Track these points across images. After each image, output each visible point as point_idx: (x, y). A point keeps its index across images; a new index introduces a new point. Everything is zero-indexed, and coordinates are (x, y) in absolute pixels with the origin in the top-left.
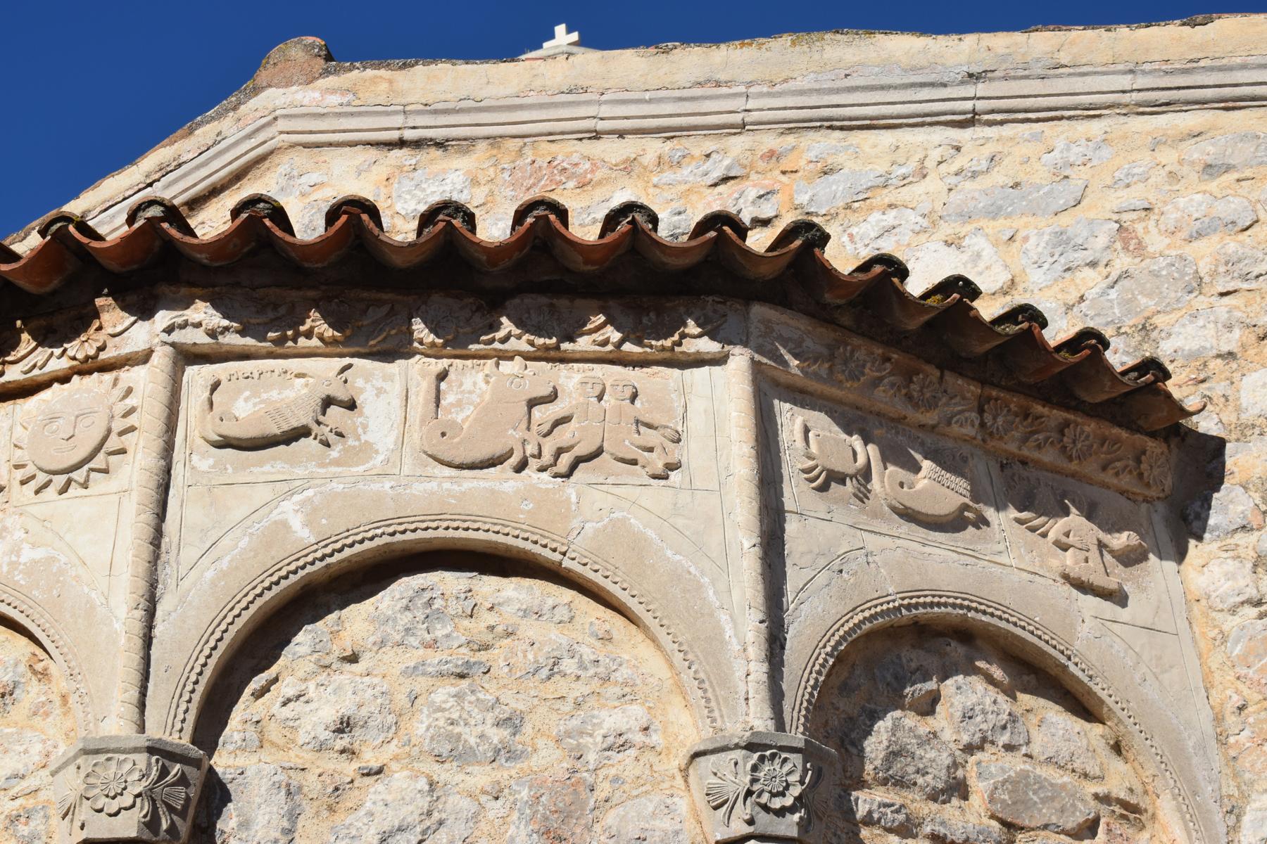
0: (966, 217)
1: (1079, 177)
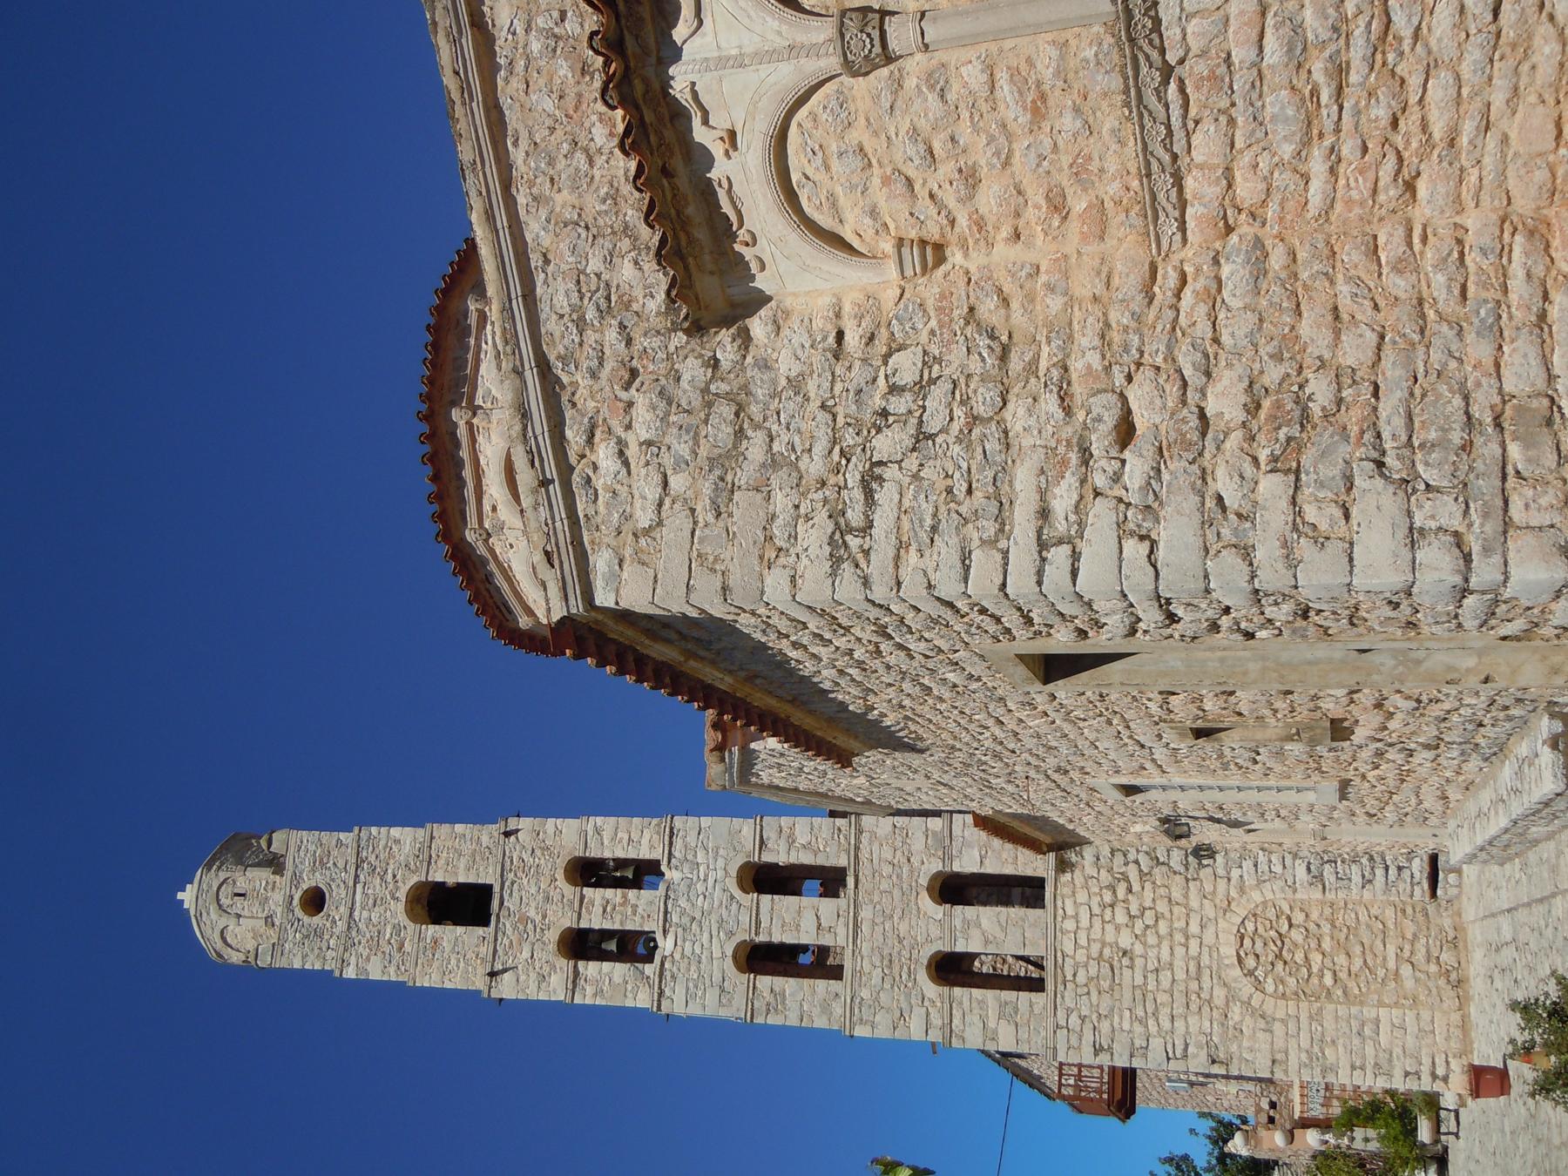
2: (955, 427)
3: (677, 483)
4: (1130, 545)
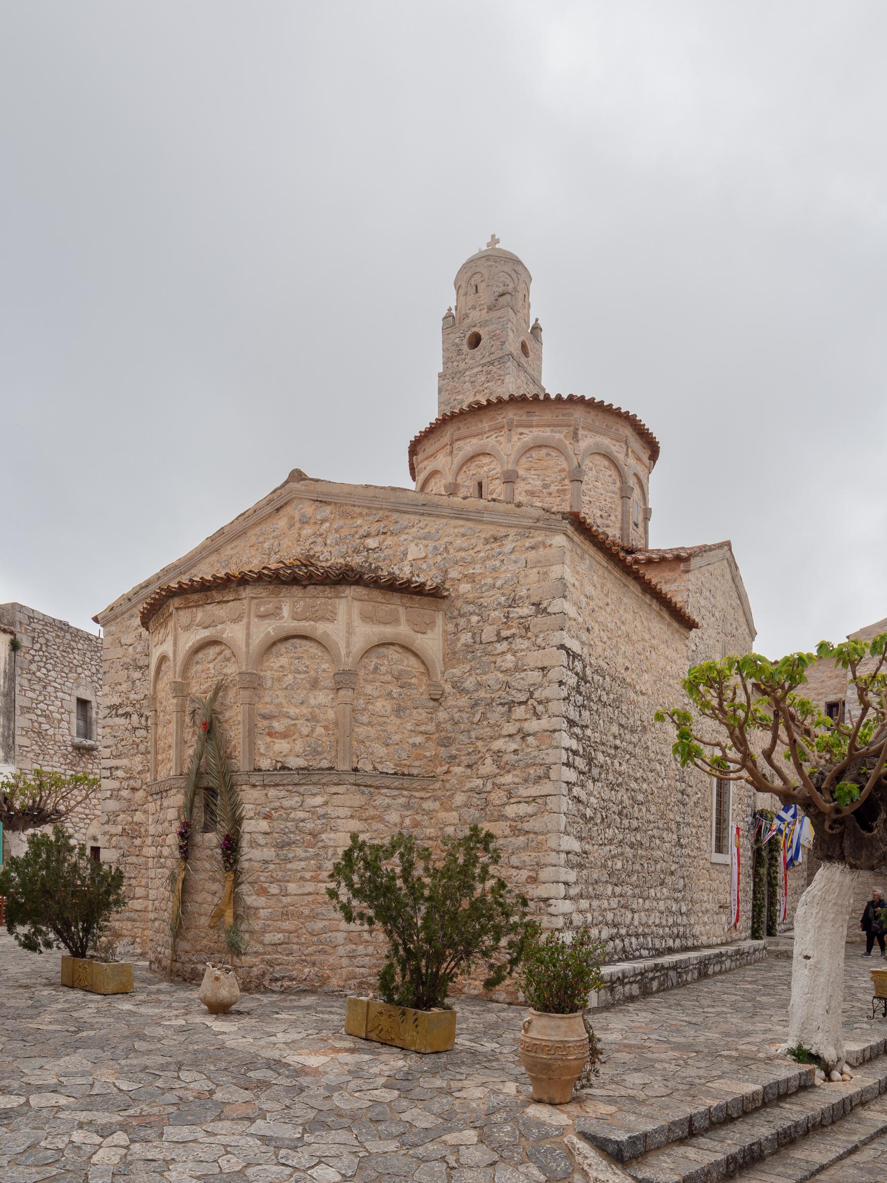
0: (420, 539)
1: (441, 532)
2: (136, 739)
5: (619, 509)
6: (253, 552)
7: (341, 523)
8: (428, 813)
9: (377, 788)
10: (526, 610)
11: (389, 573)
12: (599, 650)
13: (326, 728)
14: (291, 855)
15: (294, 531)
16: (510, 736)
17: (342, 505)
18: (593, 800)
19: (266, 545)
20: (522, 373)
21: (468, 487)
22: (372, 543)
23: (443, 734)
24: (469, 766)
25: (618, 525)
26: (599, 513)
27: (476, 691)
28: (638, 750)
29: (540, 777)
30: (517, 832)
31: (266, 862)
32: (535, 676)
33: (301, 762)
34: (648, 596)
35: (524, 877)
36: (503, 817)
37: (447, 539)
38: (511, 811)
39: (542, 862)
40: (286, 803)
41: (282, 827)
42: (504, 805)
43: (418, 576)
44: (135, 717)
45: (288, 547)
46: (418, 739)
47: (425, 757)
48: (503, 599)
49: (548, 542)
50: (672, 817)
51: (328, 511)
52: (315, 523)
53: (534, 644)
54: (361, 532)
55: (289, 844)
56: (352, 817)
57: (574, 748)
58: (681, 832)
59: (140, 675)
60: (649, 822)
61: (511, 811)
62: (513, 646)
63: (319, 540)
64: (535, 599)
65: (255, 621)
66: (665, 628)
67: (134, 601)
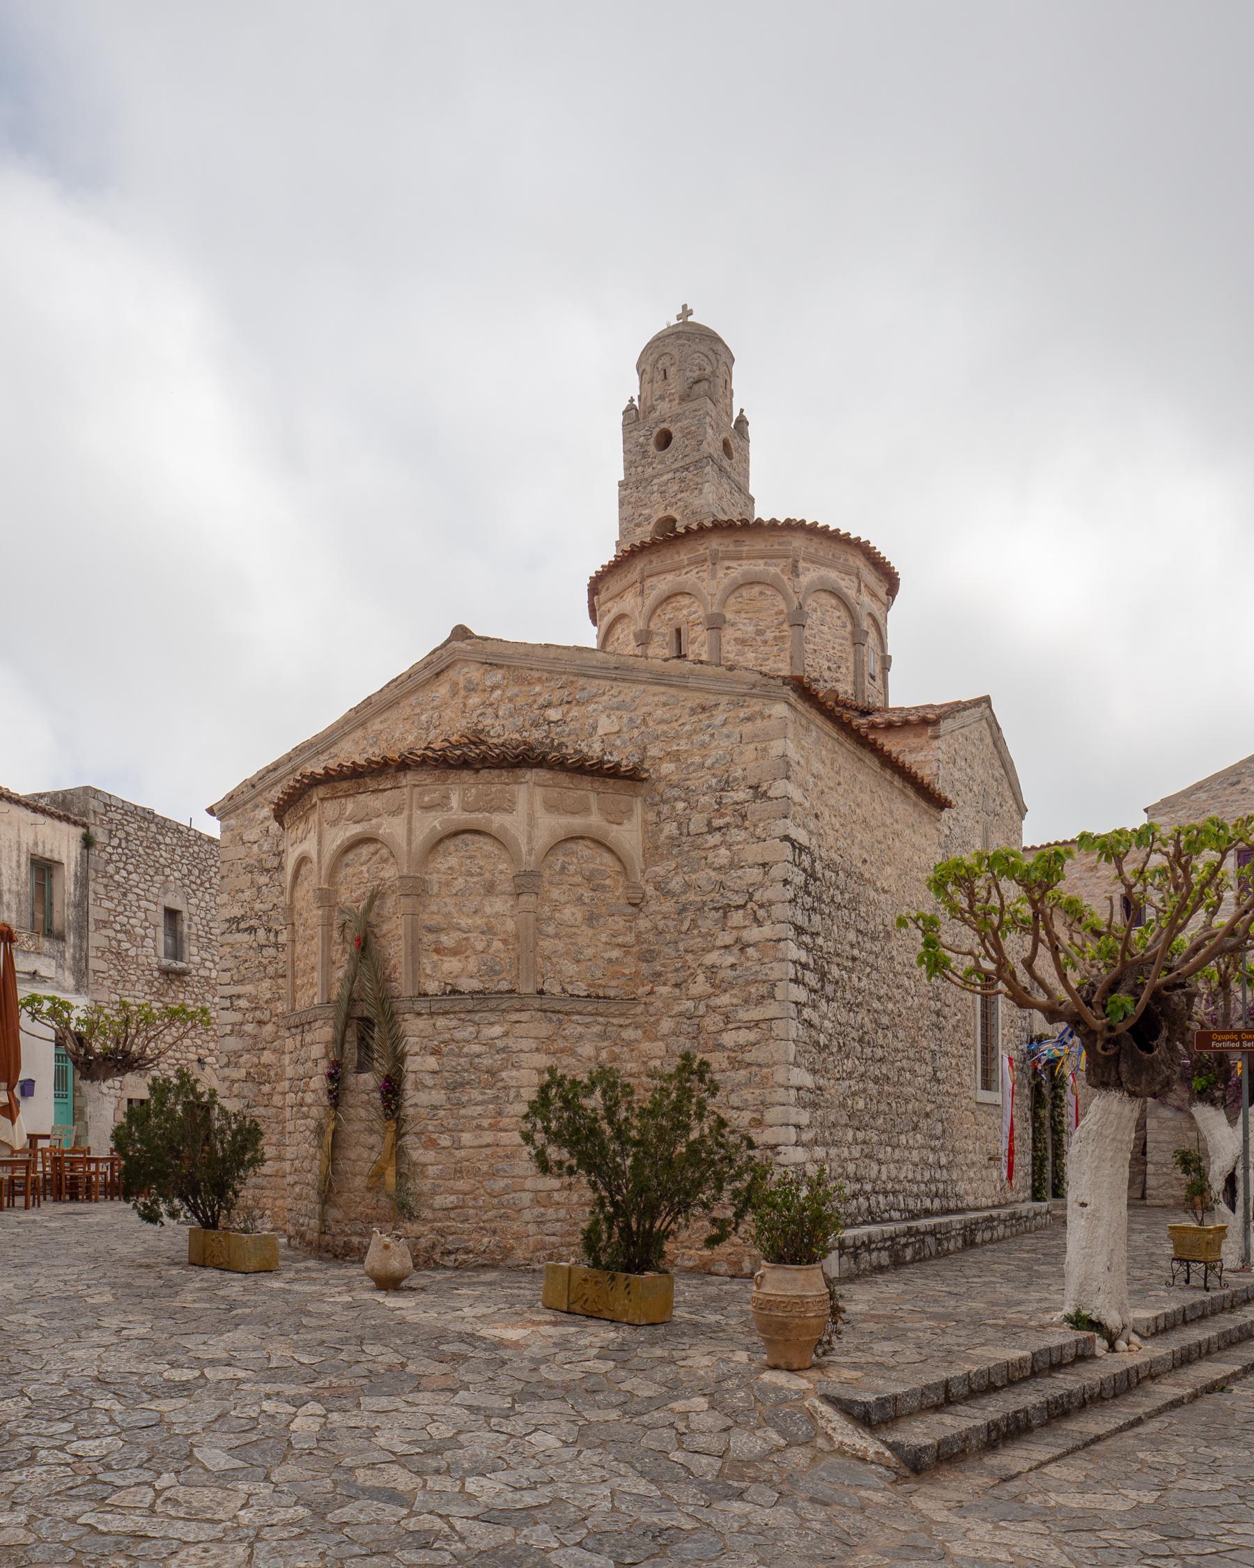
0: (612, 709)
1: (637, 701)
3: (255, 847)
4: (229, 1027)
5: (851, 658)
6: (407, 727)
7: (516, 690)
8: (629, 1043)
9: (567, 1014)
10: (742, 795)
11: (576, 752)
12: (831, 839)
13: (504, 941)
14: (465, 1099)
15: (458, 701)
16: (726, 947)
17: (516, 668)
18: (827, 1024)
19: (424, 718)
20: (724, 480)
21: (664, 635)
22: (554, 714)
23: (645, 946)
24: (677, 985)
25: (850, 679)
26: (826, 664)
27: (685, 893)
28: (881, 962)
29: (763, 997)
30: (736, 1064)
31: (435, 1108)
32: (754, 874)
33: (475, 985)
34: (889, 771)
35: (746, 1120)
36: (720, 1047)
37: (645, 709)
38: (728, 1039)
39: (768, 1100)
40: (459, 1035)
41: (454, 1064)
42: (720, 1032)
43: (611, 754)
44: (261, 932)
45: (451, 719)
46: (615, 954)
47: (624, 975)
48: (714, 781)
49: (767, 712)
50: (925, 1044)
51: (500, 676)
52: (484, 691)
53: (753, 835)
54: (541, 701)
55: (462, 1085)
56: (537, 1050)
57: (803, 960)
58: (938, 1064)
59: (267, 880)
60: (897, 1050)
61: (728, 1039)
62: (728, 838)
63: (490, 710)
64: (754, 782)
65: (417, 813)
66: (910, 809)
67: (259, 787)
